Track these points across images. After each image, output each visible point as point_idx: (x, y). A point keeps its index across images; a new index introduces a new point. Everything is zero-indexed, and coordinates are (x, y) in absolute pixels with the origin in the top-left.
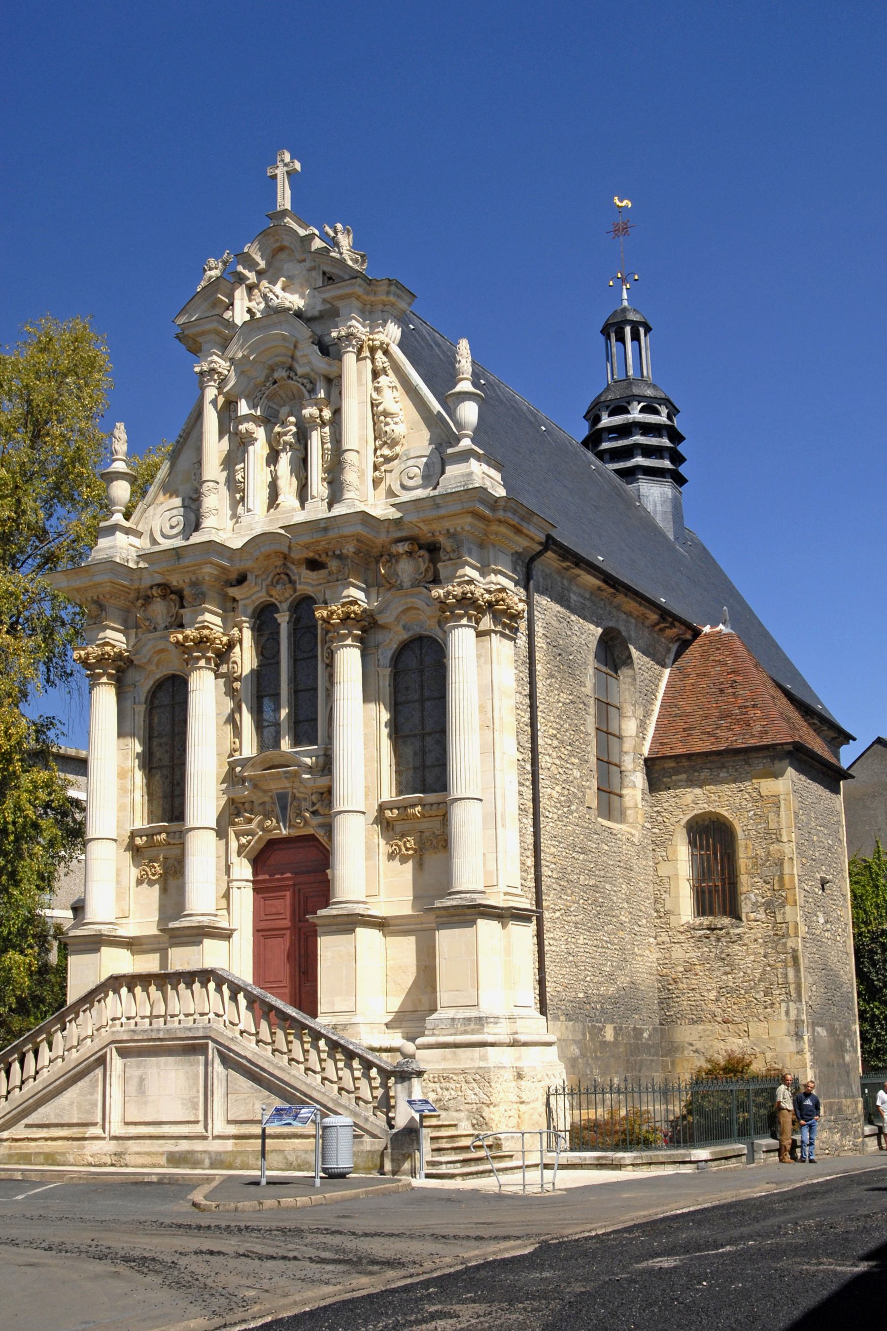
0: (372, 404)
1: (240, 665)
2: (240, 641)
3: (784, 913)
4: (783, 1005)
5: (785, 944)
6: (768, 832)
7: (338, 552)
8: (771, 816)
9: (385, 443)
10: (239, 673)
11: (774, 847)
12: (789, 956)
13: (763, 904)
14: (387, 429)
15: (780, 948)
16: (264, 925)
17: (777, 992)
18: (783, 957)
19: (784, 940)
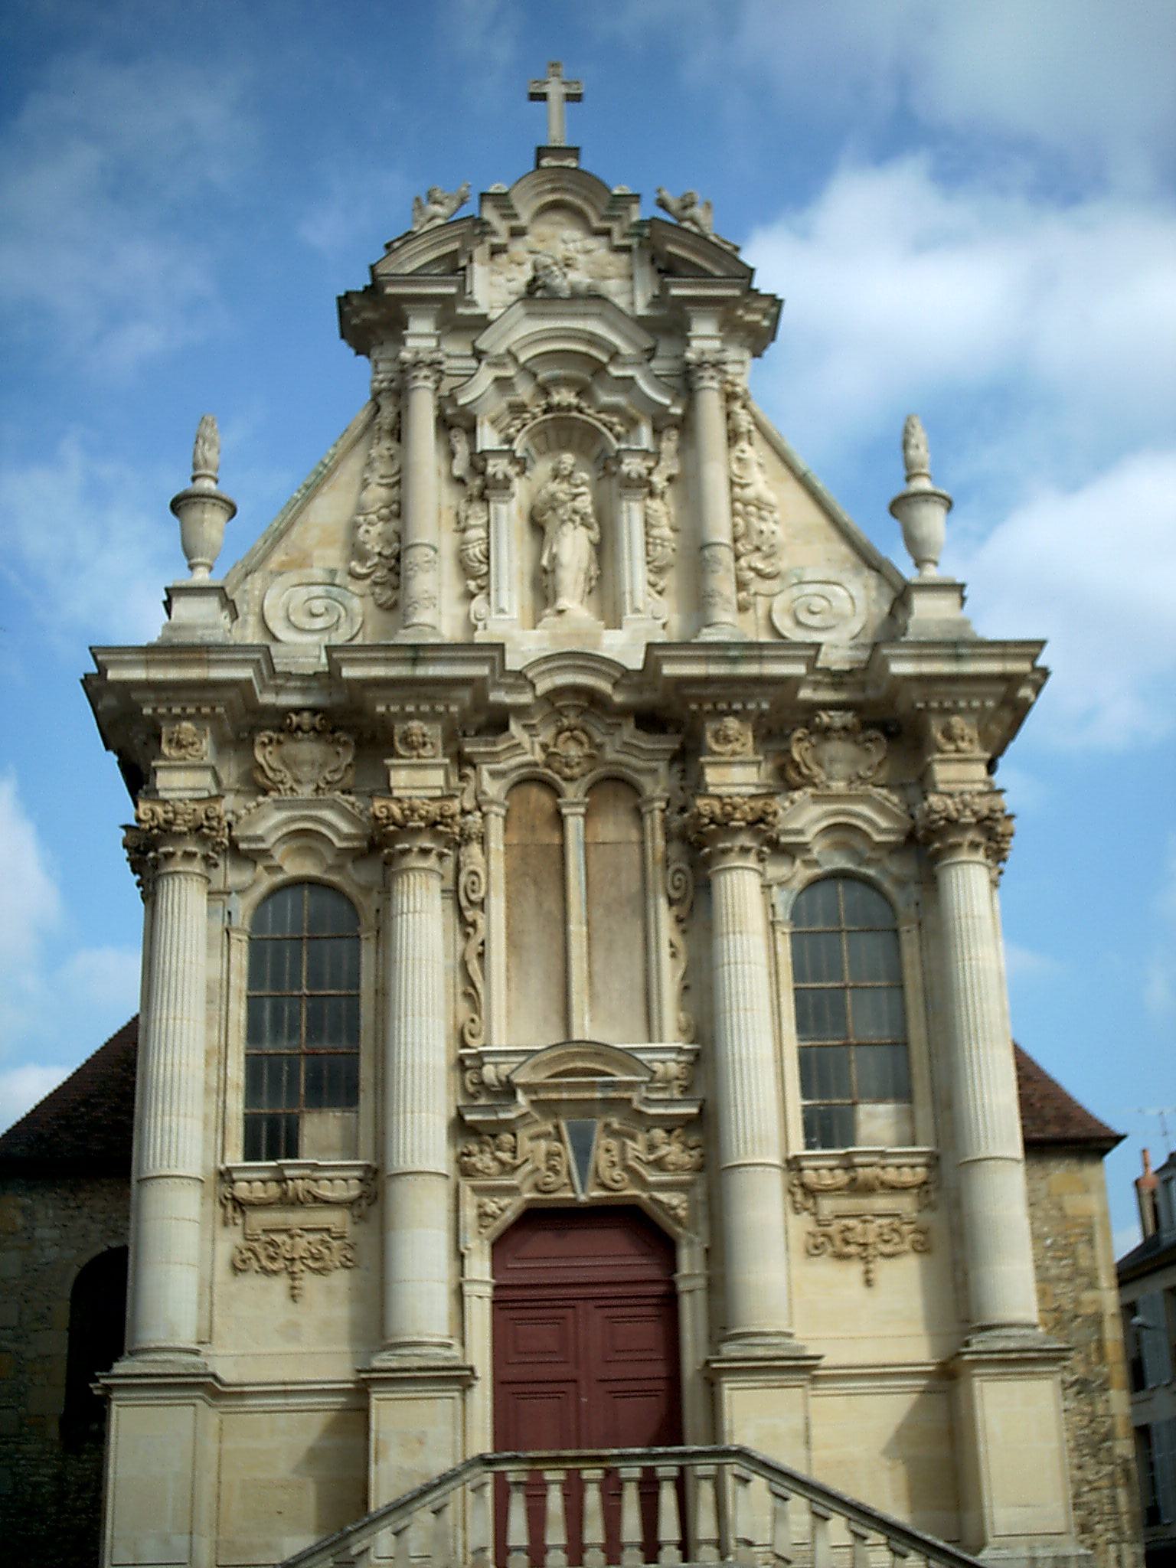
0: (732, 484)
1: (483, 880)
2: (483, 840)
3: (1107, 1401)
4: (1112, 1548)
5: (1110, 1450)
6: (1077, 1272)
7: (737, 706)
8: (1082, 1248)
9: (758, 549)
10: (482, 894)
11: (1087, 1296)
12: (1119, 1469)
13: (1073, 1384)
14: (763, 526)
15: (1102, 1455)
16: (513, 1373)
17: (1099, 1527)
18: (1109, 1468)
19: (1108, 1444)
